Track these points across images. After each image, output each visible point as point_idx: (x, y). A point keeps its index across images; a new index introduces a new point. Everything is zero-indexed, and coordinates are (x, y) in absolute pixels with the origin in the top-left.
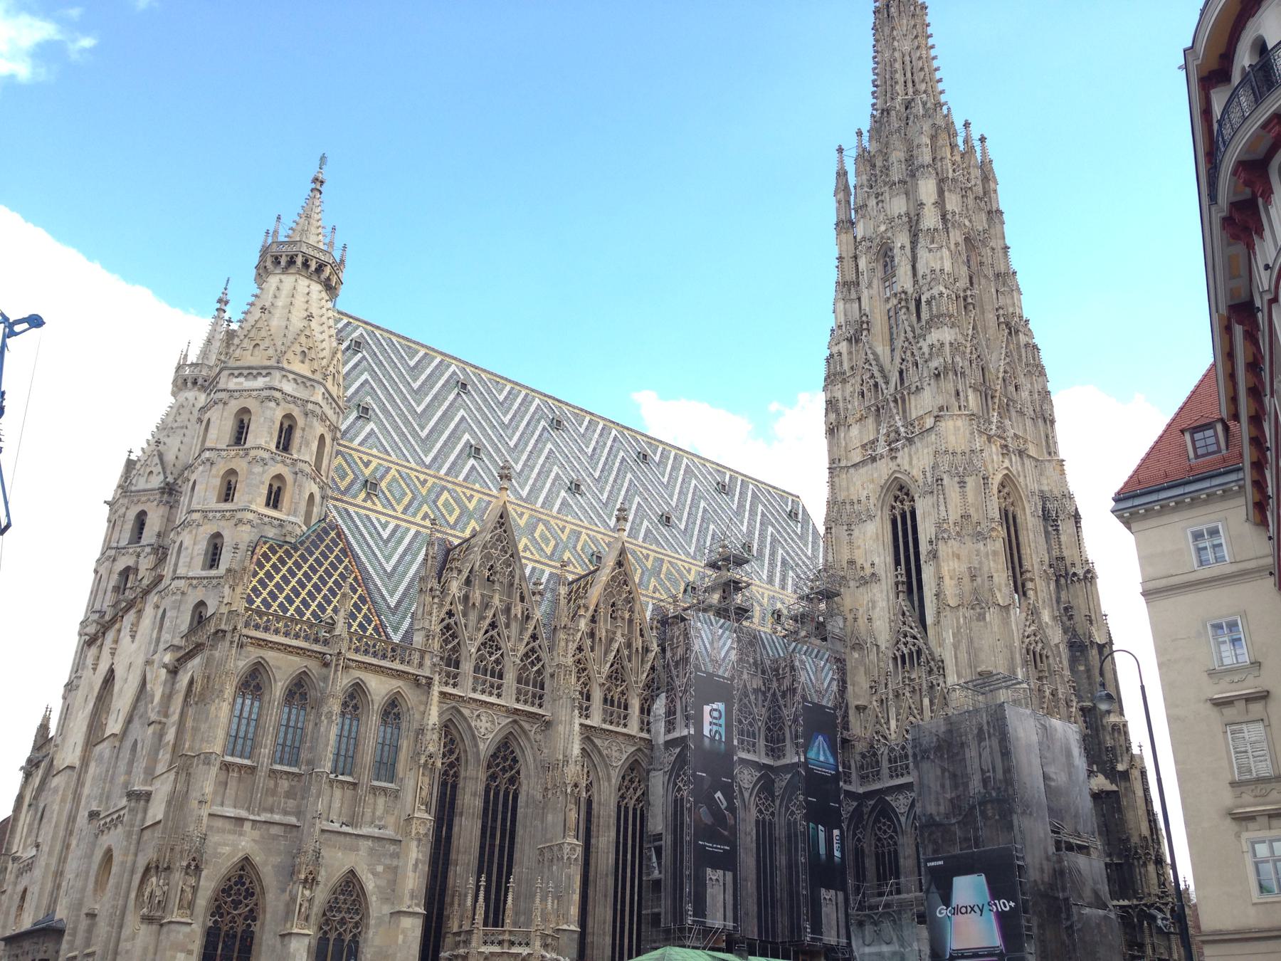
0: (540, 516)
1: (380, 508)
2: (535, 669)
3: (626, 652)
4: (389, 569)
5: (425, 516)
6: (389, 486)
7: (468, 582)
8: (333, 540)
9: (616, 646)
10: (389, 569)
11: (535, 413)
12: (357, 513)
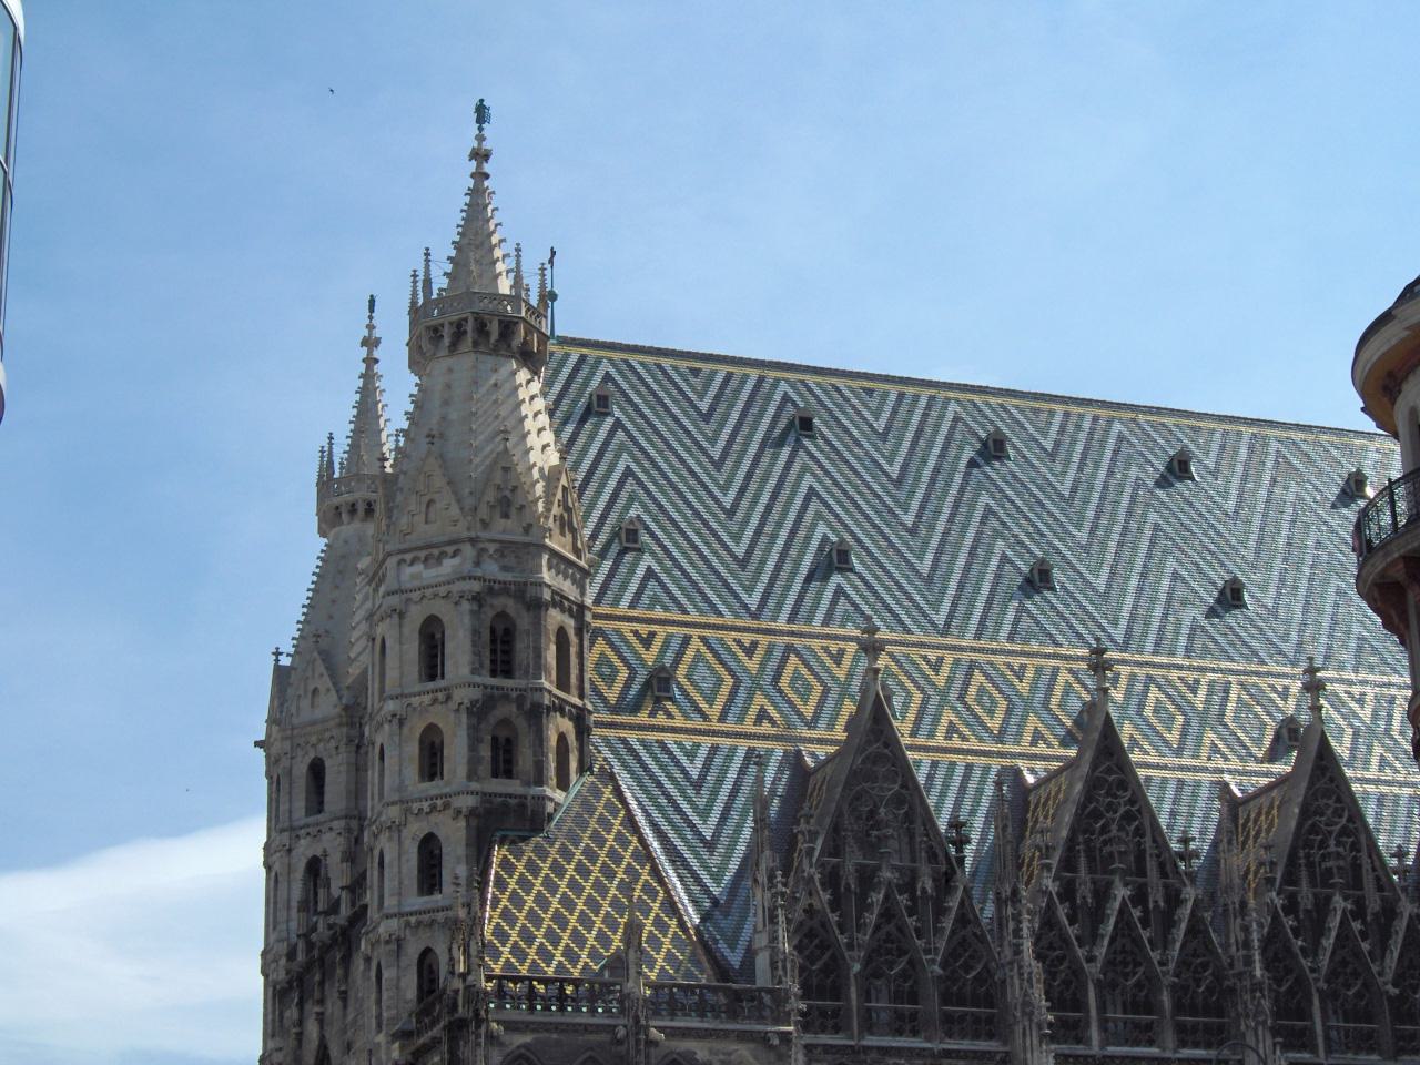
0: (974, 656)
1: (679, 722)
2: (974, 973)
3: (1137, 913)
4: (708, 834)
5: (762, 716)
6: (689, 677)
7: (835, 848)
8: (609, 804)
9: (1117, 905)
10: (708, 834)
11: (948, 440)
12: (642, 742)
